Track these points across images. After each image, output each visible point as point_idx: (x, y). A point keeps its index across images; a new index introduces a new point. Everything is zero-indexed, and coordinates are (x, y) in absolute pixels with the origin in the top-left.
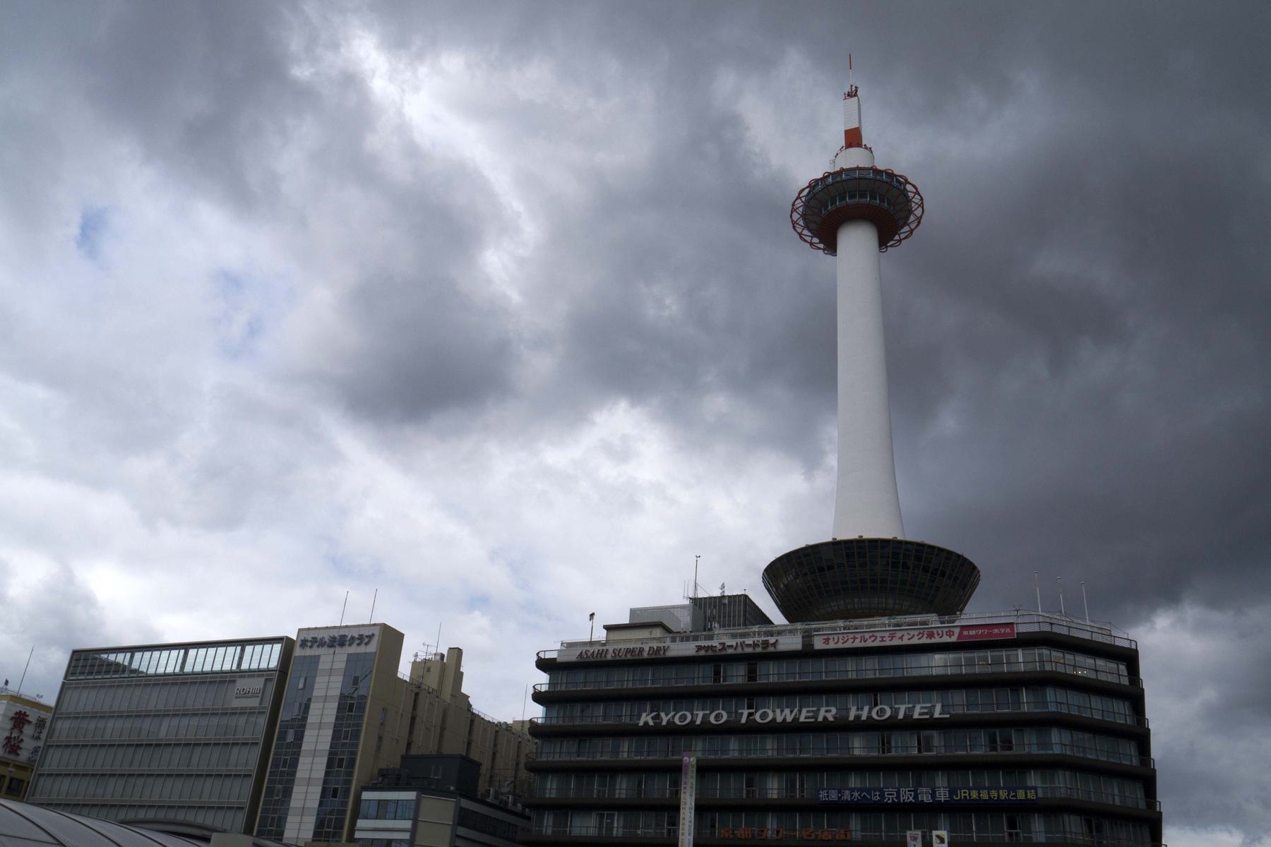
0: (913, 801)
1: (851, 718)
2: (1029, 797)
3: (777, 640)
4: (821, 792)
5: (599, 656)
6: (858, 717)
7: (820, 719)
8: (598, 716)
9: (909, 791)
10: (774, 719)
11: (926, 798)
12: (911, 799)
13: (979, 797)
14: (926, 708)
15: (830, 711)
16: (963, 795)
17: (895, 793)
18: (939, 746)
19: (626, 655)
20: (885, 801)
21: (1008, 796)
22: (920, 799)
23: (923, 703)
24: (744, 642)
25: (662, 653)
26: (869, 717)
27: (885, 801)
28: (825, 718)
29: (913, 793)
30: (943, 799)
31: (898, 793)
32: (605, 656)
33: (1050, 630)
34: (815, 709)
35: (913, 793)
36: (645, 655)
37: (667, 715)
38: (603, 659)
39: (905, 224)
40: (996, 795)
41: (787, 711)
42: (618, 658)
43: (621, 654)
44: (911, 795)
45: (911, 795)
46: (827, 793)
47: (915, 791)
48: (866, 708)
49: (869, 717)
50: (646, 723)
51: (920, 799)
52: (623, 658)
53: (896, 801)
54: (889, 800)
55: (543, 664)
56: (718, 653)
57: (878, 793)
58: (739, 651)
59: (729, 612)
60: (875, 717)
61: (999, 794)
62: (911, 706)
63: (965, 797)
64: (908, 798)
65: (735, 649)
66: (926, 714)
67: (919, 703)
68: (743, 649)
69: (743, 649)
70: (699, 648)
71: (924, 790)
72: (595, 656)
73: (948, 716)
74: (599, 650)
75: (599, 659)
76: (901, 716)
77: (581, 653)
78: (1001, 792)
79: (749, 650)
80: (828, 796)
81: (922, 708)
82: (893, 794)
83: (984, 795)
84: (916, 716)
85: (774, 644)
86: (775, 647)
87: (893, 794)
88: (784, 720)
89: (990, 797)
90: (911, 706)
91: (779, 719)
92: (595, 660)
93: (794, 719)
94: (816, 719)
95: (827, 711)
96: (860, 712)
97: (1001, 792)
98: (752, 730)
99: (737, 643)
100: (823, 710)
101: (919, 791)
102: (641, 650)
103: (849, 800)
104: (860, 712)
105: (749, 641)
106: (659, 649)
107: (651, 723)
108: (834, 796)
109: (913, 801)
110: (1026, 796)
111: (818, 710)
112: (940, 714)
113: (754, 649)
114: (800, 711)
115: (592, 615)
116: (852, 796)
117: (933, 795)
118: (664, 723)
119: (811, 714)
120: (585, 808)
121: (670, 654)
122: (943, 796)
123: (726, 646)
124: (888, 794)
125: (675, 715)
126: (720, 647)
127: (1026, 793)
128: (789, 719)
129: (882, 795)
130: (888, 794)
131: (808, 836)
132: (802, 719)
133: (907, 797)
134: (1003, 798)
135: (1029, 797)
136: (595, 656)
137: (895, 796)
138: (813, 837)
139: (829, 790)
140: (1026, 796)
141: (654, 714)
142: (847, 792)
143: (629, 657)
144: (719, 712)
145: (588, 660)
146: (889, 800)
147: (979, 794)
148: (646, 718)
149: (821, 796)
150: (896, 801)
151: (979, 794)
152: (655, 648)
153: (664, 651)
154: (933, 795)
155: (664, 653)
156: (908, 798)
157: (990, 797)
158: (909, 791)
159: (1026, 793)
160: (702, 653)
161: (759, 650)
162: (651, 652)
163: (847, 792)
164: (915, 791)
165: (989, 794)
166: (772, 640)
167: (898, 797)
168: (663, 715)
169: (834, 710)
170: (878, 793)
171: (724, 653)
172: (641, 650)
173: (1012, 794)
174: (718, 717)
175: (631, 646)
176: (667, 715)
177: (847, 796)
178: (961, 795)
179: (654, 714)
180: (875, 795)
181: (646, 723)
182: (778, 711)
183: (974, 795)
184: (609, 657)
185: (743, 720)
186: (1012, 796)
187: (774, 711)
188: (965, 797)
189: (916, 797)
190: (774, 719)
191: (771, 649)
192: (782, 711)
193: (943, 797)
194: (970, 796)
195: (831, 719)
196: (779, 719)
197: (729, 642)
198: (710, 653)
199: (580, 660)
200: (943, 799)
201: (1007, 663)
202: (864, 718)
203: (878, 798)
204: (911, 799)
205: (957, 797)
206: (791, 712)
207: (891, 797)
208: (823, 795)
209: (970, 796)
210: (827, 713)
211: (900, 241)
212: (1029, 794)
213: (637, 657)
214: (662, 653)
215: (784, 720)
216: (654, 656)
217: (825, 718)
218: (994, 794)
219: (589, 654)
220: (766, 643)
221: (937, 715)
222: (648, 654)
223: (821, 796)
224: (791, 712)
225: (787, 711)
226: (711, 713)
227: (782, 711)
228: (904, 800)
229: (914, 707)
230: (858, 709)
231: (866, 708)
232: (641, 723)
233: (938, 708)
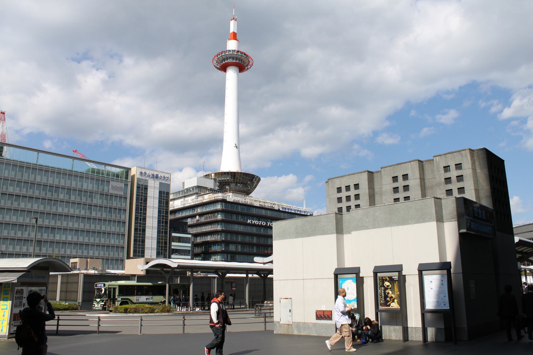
8: (234, 218)
37: (254, 221)
50: (249, 222)
107: (250, 223)
118: (253, 223)
126: (263, 206)
141: (251, 220)
148: (249, 221)
166: (273, 206)
168: (253, 221)
174: (264, 223)
176: (254, 221)
179: (251, 220)
181: (249, 222)
185: (268, 225)
232: (248, 222)
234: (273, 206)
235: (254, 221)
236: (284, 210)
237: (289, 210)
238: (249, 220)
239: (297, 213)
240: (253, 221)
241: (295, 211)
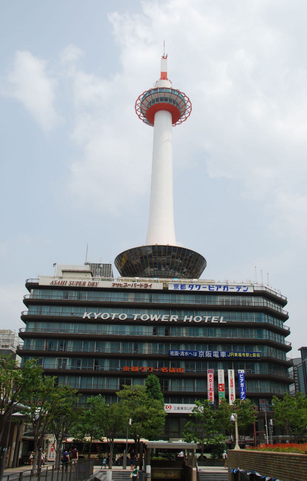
0: (211, 357)
1: (185, 321)
2: (257, 356)
3: (152, 284)
4: (171, 352)
5: (62, 283)
6: (188, 321)
7: (171, 320)
9: (209, 352)
10: (150, 319)
11: (216, 355)
12: (210, 356)
13: (238, 355)
14: (216, 318)
15: (175, 317)
16: (231, 355)
17: (203, 353)
18: (218, 334)
19: (76, 284)
20: (199, 356)
21: (249, 355)
22: (214, 356)
23: (165, 315)
24: (136, 284)
25: (95, 285)
26: (193, 321)
27: (199, 356)
28: (173, 320)
29: (211, 353)
30: (223, 356)
31: (205, 353)
32: (66, 284)
33: (265, 290)
34: (218, 317)
35: (211, 353)
36: (86, 285)
37: (97, 314)
38: (64, 285)
39: (184, 114)
40: (245, 355)
41: (156, 316)
42: (72, 286)
43: (74, 284)
44: (210, 354)
45: (210, 354)
46: (174, 352)
47: (212, 353)
48: (191, 317)
49: (193, 321)
50: (87, 317)
51: (214, 356)
52: (75, 286)
53: (204, 356)
54: (201, 356)
55: (30, 286)
56: (123, 287)
57: (196, 353)
58: (133, 287)
59: (103, 271)
60: (195, 320)
61: (246, 355)
62: (211, 317)
63: (232, 355)
64: (209, 356)
65: (132, 286)
66: (167, 319)
67: (164, 315)
68: (135, 286)
69: (135, 286)
70: (114, 284)
71: (216, 352)
72: (60, 283)
73: (226, 322)
74: (62, 281)
75: (62, 285)
76: (206, 321)
77: (53, 281)
78: (246, 354)
79: (138, 287)
80: (174, 354)
81: (215, 318)
82: (203, 354)
83: (240, 355)
84: (212, 321)
85: (151, 286)
86: (151, 287)
87: (203, 354)
88: (154, 320)
89: (242, 356)
90: (211, 317)
91: (152, 319)
92: (60, 285)
93: (159, 320)
94: (169, 320)
95: (174, 317)
96: (188, 318)
97: (246, 354)
98: (139, 323)
99: (133, 284)
100: (172, 316)
101: (213, 353)
102: (84, 283)
103: (183, 355)
104: (188, 318)
105: (139, 283)
106: (93, 284)
107: (89, 317)
108: (177, 354)
109: (211, 357)
110: (256, 355)
111: (170, 316)
112: (223, 321)
113: (141, 287)
114: (162, 316)
115: (55, 264)
116: (185, 354)
117: (219, 354)
118: (96, 318)
119: (167, 318)
120: (51, 355)
121: (99, 286)
122: (223, 354)
123: (127, 285)
124: (200, 354)
125: (101, 314)
127: (256, 355)
128: (157, 320)
129: (198, 354)
130: (200, 354)
131: (165, 371)
132: (163, 320)
133: (208, 354)
134: (247, 356)
135: (257, 356)
136: (60, 283)
137: (203, 354)
138: (167, 371)
139: (174, 351)
140: (256, 355)
141: (90, 313)
142: (183, 352)
143: (78, 285)
144: (146, 315)
145: (56, 285)
146: (201, 356)
147: (238, 354)
149: (171, 353)
150: (204, 356)
151: (238, 354)
152: (92, 283)
153: (97, 284)
154: (219, 354)
155: (96, 285)
156: (209, 356)
157: (242, 356)
158: (209, 352)
159: (256, 355)
160: (115, 287)
161: (143, 288)
162: (90, 284)
163: (183, 352)
164: (212, 353)
165: (242, 355)
167: (205, 355)
168: (95, 314)
169: (177, 317)
170: (196, 353)
171: (126, 287)
172: (84, 283)
173: (251, 355)
174: (123, 317)
175: (79, 281)
177: (182, 354)
178: (231, 354)
179: (90, 313)
180: (195, 354)
181: (87, 317)
182: (152, 316)
183: (236, 355)
184: (67, 285)
185: (135, 319)
186: (251, 356)
187: (150, 316)
188: (232, 355)
189: (212, 355)
190: (150, 319)
191: (148, 288)
192: (153, 316)
193: (223, 355)
194: (234, 355)
195: (176, 320)
196: (152, 319)
197: (128, 283)
198: (119, 287)
199: (51, 285)
200: (223, 356)
201: (246, 302)
202: (190, 321)
203: (196, 355)
204: (210, 356)
205: (229, 355)
206: (158, 316)
207: (201, 355)
208: (172, 353)
209: (234, 355)
210: (174, 318)
211: (182, 122)
212: (257, 355)
213: (82, 286)
214: (95, 285)
215: (154, 320)
216: (91, 286)
217: (173, 320)
218: (244, 354)
219: (57, 282)
220: (146, 285)
221: (221, 321)
222: (88, 285)
223: (171, 353)
224: (158, 316)
225: (156, 316)
226: (119, 315)
227: (153, 316)
228: (207, 356)
229: (212, 318)
230: (188, 317)
231: (191, 317)
232: (84, 317)
233: (222, 318)
234: (149, 284)
235: (100, 314)
236: (180, 289)
237: (192, 288)
238: (86, 313)
239: (215, 290)
240: (95, 314)
241: (209, 287)
